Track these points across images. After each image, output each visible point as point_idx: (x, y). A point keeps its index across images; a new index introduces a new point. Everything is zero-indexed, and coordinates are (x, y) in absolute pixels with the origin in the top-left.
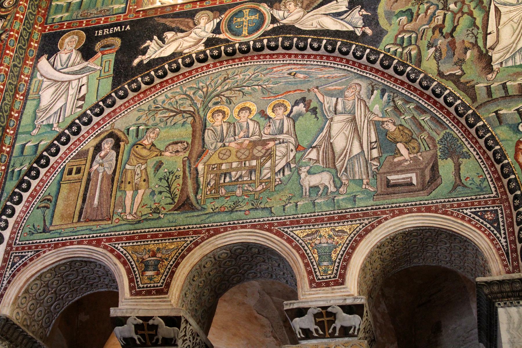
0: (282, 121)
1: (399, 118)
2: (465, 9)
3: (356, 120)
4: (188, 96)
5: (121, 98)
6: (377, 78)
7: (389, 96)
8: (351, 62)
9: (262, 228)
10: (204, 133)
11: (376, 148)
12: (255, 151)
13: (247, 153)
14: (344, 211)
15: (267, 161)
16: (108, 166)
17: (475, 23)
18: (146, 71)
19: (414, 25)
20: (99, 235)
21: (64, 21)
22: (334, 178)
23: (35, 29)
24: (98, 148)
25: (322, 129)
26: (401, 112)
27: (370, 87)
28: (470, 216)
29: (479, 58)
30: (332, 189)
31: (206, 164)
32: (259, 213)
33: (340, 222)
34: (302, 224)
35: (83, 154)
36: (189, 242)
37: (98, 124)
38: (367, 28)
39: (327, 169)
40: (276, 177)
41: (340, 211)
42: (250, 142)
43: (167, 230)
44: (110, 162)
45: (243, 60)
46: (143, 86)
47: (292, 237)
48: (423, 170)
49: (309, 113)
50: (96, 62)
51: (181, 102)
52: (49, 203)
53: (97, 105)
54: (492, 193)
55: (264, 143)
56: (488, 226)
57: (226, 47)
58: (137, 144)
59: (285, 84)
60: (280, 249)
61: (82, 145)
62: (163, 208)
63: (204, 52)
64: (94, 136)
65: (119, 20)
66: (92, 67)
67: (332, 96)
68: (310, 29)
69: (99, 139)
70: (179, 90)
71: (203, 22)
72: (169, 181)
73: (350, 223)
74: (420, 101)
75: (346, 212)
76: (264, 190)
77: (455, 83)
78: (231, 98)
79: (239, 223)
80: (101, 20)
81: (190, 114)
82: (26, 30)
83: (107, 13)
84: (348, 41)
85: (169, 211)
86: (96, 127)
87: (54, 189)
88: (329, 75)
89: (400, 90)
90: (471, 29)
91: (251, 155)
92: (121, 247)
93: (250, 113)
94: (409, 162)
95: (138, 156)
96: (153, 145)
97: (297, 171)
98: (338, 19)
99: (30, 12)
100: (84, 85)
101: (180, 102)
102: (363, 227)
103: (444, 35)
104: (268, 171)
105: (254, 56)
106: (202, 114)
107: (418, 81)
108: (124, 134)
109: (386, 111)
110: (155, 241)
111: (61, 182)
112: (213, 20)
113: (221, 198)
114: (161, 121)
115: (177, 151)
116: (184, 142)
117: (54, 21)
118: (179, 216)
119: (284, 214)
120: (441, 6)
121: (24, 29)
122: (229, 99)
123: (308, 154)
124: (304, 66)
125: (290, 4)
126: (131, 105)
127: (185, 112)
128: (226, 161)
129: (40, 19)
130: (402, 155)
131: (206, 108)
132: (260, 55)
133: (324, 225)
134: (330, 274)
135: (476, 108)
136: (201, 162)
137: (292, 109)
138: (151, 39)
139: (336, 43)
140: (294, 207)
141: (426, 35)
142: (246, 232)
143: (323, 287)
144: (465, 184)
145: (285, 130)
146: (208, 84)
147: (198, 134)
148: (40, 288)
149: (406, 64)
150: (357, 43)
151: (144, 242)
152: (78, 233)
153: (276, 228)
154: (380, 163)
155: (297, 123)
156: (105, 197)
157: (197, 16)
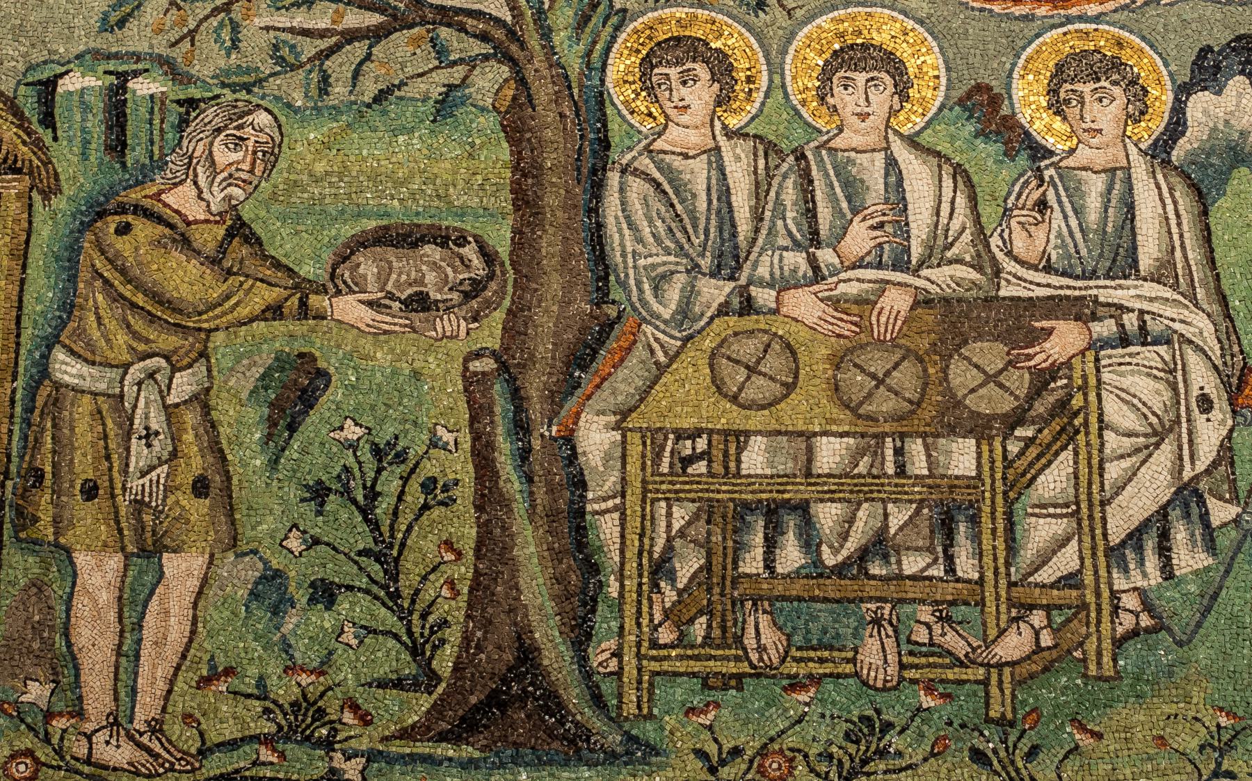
0: (1118, 175)
10: (597, 188)
12: (961, 376)
13: (906, 378)
15: (1047, 455)
31: (633, 422)
40: (1120, 583)
42: (923, 302)
58: (122, 209)
62: (355, 708)
72: (382, 508)
81: (484, 37)
93: (902, 91)
95: (140, 299)
96: (239, 230)
104: (1059, 527)
116: (462, 241)
136: (595, 403)
145: (1148, 255)
155: (1222, 210)
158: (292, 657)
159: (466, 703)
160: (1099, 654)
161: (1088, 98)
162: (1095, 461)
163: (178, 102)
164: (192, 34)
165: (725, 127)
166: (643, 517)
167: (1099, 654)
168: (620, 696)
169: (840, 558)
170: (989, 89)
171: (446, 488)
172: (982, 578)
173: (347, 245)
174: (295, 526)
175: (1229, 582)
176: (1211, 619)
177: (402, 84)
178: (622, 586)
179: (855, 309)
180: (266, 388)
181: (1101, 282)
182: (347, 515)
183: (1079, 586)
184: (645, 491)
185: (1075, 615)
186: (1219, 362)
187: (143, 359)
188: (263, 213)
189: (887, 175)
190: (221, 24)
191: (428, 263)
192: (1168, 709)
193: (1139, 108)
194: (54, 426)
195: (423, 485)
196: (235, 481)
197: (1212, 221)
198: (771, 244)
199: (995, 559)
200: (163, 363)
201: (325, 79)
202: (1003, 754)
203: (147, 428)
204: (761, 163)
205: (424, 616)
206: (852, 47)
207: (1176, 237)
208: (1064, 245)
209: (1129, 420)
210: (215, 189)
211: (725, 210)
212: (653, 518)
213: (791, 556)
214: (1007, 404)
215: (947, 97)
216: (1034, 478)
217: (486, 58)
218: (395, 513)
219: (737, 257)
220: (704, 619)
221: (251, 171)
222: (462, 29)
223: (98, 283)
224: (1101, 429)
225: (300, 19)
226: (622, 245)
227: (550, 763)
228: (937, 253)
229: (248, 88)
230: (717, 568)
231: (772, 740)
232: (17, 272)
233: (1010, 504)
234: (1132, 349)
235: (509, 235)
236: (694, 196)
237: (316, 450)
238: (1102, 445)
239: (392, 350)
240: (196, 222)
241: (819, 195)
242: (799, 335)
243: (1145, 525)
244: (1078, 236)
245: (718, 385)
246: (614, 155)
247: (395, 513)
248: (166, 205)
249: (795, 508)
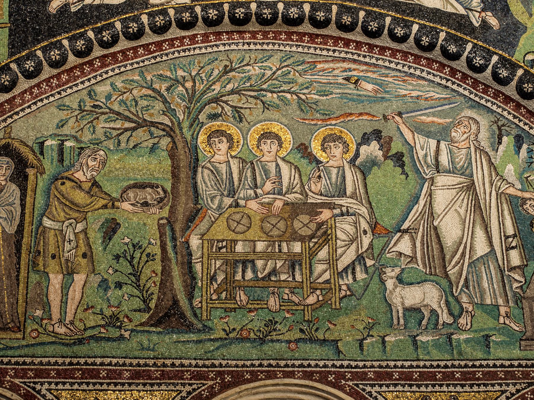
0: (341, 169)
3: (475, 189)
4: (159, 92)
8: (459, 75)
9: (323, 378)
10: (195, 172)
12: (297, 225)
13: (281, 225)
14: (470, 364)
15: (321, 247)
16: (5, 216)
22: (447, 297)
25: (416, 199)
27: (495, 127)
30: (445, 317)
34: (396, 379)
40: (341, 282)
41: (463, 363)
42: (286, 204)
43: (139, 365)
45: (259, 36)
49: (389, 161)
51: (145, 103)
58: (62, 178)
62: (127, 317)
67: (428, 135)
70: (137, 78)
72: (135, 261)
75: (474, 366)
76: (320, 305)
78: (242, 111)
81: (164, 130)
88: (420, 93)
92: (49, 390)
93: (280, 145)
95: (67, 203)
96: (95, 184)
101: (143, 103)
104: (324, 267)
105: (280, 33)
108: (33, 151)
110: (116, 384)
114: (109, 138)
116: (157, 187)
122: (238, 112)
124: (371, 69)
126: (43, 94)
131: (195, 123)
132: (293, 33)
133: (437, 388)
137: (358, 150)
140: (380, 346)
142: (296, 385)
145: (349, 190)
146: (193, 74)
151: (94, 384)
153: (351, 383)
154: (524, 277)
158: (110, 303)
159: (159, 315)
160: (335, 302)
161: (332, 147)
162: (334, 248)
163: (78, 148)
164: (82, 129)
165: (231, 155)
166: (208, 264)
167: (335, 302)
168: (202, 314)
169: (263, 275)
170: (305, 144)
171: (153, 256)
172: (303, 281)
173: (125, 188)
174: (111, 266)
175: (372, 282)
176: (367, 292)
177: (141, 143)
178: (202, 283)
179: (267, 206)
180: (103, 228)
181: (336, 198)
182: (125, 263)
183: (330, 283)
184: (209, 257)
185: (329, 291)
186: (369, 221)
187: (68, 220)
188: (102, 179)
189: (276, 168)
190: (90, 126)
191: (148, 193)
192: (355, 318)
193: (346, 150)
194: (44, 238)
195: (146, 255)
196: (94, 254)
197: (367, 181)
198: (244, 188)
199: (306, 276)
200: (74, 221)
201: (119, 142)
202: (308, 330)
203: (69, 239)
204: (241, 165)
205: (147, 292)
206: (266, 133)
207: (357, 186)
208: (326, 188)
209: (344, 237)
210: (88, 172)
211: (231, 178)
212: (211, 264)
213: (249, 275)
214: (310, 233)
215: (293, 147)
216: (317, 253)
217: (164, 136)
218: (139, 263)
219: (234, 192)
220: (225, 292)
221: (99, 167)
222: (157, 128)
223: (56, 199)
224: (336, 239)
225: (112, 125)
226: (202, 188)
227: (182, 333)
228: (290, 190)
229: (98, 144)
230: (229, 278)
231: (244, 326)
232: (33, 195)
233: (310, 260)
234: (345, 217)
235: (170, 185)
236: (222, 174)
237: (116, 245)
238: (336, 244)
239: (138, 217)
240: (83, 182)
241: (257, 174)
242: (252, 213)
243: (348, 266)
244: (330, 185)
245: (229, 227)
246: (200, 163)
247: (139, 263)
248: (75, 177)
249: (250, 261)
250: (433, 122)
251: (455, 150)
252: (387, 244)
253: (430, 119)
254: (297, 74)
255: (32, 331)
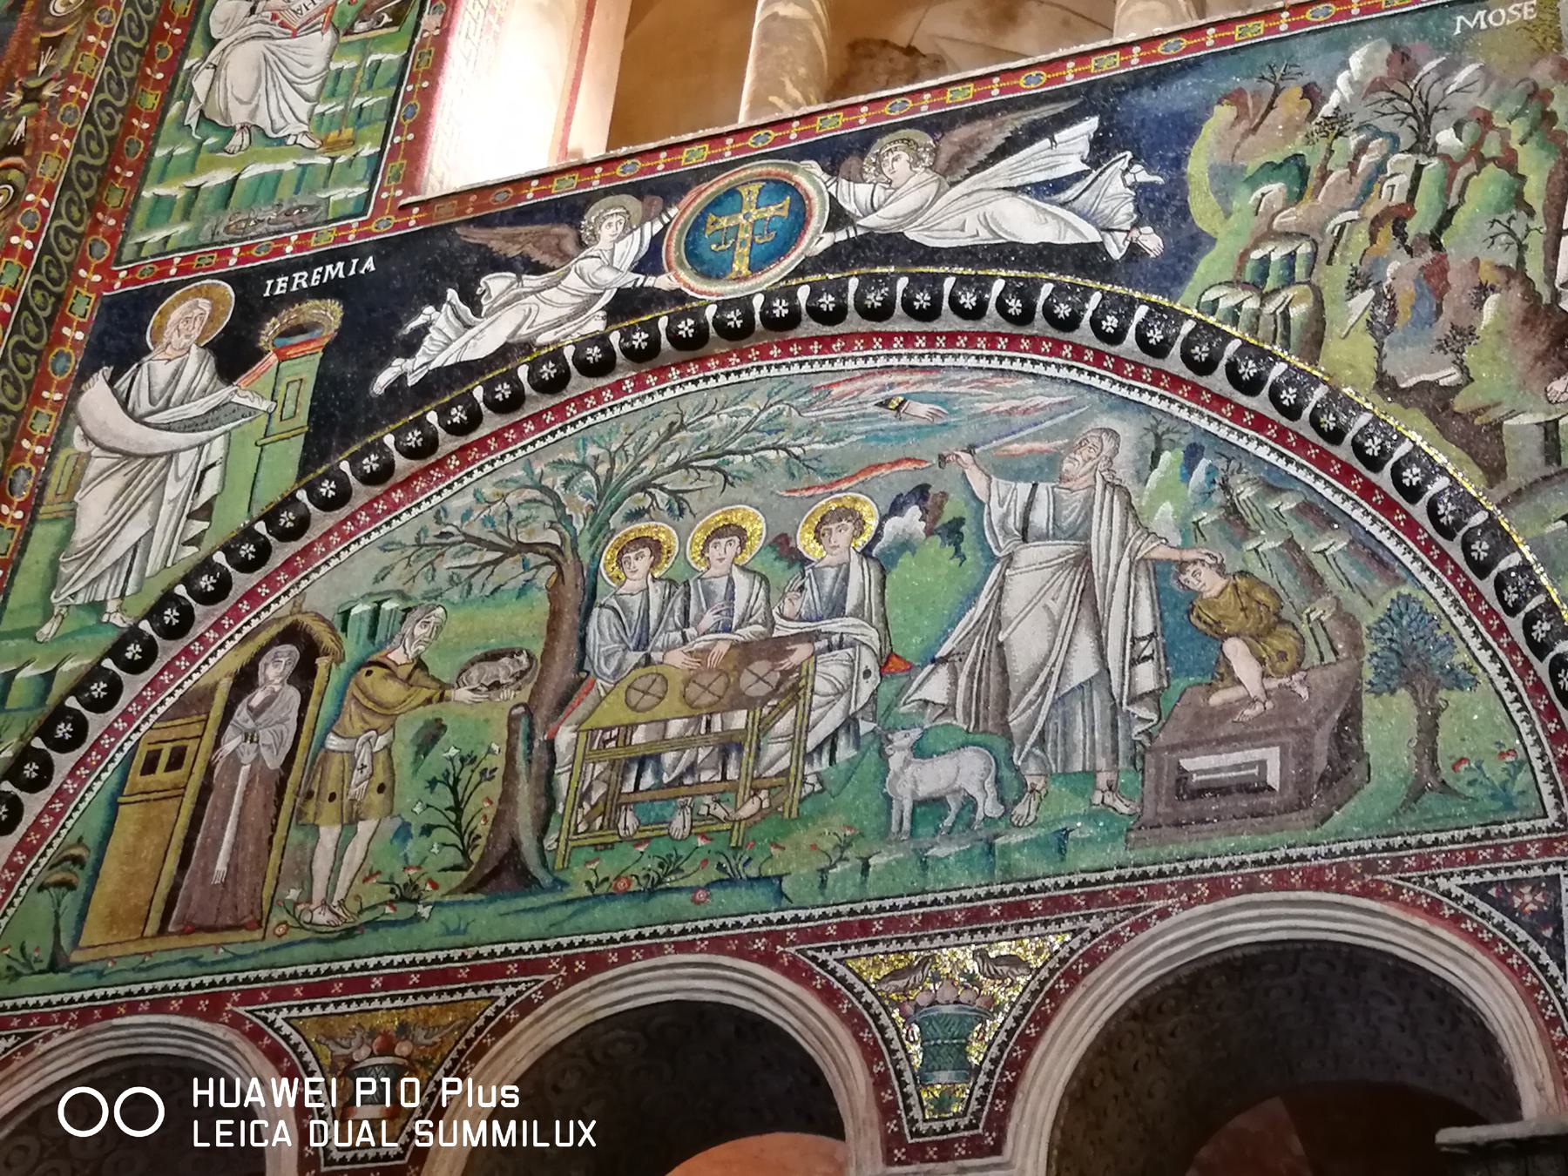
1: (1239, 547)
2: (1492, 148)
5: (327, 505)
6: (1174, 408)
7: (1211, 470)
8: (1089, 356)
10: (586, 616)
11: (1151, 657)
12: (747, 679)
13: (718, 686)
15: (783, 711)
17: (1519, 195)
18: (412, 412)
19: (1308, 211)
20: (219, 979)
21: (173, 252)
23: (80, 281)
24: (246, 680)
26: (1247, 525)
28: (1459, 899)
29: (1525, 322)
30: (988, 807)
31: (584, 727)
32: (740, 898)
33: (1005, 928)
35: (195, 702)
36: (501, 1003)
37: (252, 596)
38: (1148, 229)
39: (978, 738)
40: (808, 770)
41: (1008, 888)
44: (278, 728)
45: (734, 359)
46: (400, 461)
47: (842, 980)
48: (1305, 734)
49: (937, 539)
50: (258, 385)
51: (523, 513)
52: (76, 869)
53: (248, 534)
54: (1546, 816)
55: (776, 648)
56: (1522, 935)
57: (674, 319)
59: (867, 440)
60: (797, 1024)
61: (198, 670)
63: (601, 339)
64: (238, 637)
65: (345, 239)
66: (247, 402)
67: (1018, 476)
68: (954, 244)
69: (251, 648)
71: (606, 233)
72: (460, 789)
73: (1039, 929)
74: (1319, 486)
75: (1030, 890)
77: (1432, 415)
78: (686, 496)
79: (669, 934)
80: (287, 240)
81: (547, 555)
82: (45, 288)
83: (310, 218)
84: (1079, 281)
85: (450, 893)
86: (245, 606)
87: (97, 820)
89: (1252, 447)
90: (1504, 218)
91: (731, 692)
92: (286, 1020)
93: (742, 546)
94: (1259, 708)
95: (370, 705)
96: (420, 664)
97: (876, 746)
98: (1052, 203)
99: (63, 228)
100: (213, 465)
101: (521, 514)
102: (1083, 941)
103: (1408, 243)
106: (585, 552)
107: (1307, 412)
109: (1196, 524)
111: (121, 799)
112: (641, 225)
113: (621, 848)
115: (496, 685)
116: (520, 653)
117: (143, 254)
118: (481, 909)
119: (820, 900)
120: (1407, 139)
121: (37, 285)
122: (679, 500)
123: (920, 685)
125: (895, 160)
126: (360, 529)
127: (531, 547)
128: (648, 716)
129: (97, 249)
130: (1240, 683)
131: (601, 529)
132: (791, 342)
134: (956, 1115)
135: (1499, 506)
138: (438, 301)
139: (1036, 286)
141: (1346, 247)
143: (931, 1160)
144: (1450, 782)
146: (613, 449)
147: (569, 619)
148: (40, 1161)
149: (1270, 353)
150: (1108, 287)
151: (359, 1002)
152: (154, 974)
153: (792, 950)
155: (893, 577)
156: (251, 848)
157: (591, 216)
201: (470, 586)
209: (828, 689)
241: (692, 602)
243: (825, 740)
250: (1031, 451)
251: (1064, 494)
252: (902, 690)
253: (1028, 446)
254: (794, 412)
255: (279, 924)
